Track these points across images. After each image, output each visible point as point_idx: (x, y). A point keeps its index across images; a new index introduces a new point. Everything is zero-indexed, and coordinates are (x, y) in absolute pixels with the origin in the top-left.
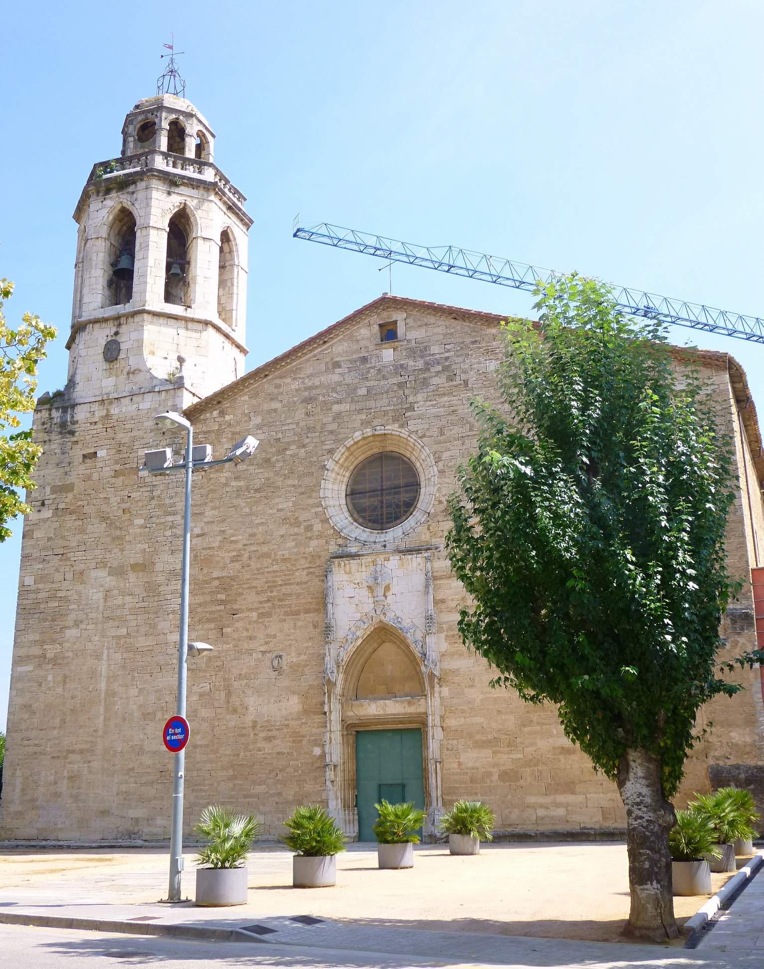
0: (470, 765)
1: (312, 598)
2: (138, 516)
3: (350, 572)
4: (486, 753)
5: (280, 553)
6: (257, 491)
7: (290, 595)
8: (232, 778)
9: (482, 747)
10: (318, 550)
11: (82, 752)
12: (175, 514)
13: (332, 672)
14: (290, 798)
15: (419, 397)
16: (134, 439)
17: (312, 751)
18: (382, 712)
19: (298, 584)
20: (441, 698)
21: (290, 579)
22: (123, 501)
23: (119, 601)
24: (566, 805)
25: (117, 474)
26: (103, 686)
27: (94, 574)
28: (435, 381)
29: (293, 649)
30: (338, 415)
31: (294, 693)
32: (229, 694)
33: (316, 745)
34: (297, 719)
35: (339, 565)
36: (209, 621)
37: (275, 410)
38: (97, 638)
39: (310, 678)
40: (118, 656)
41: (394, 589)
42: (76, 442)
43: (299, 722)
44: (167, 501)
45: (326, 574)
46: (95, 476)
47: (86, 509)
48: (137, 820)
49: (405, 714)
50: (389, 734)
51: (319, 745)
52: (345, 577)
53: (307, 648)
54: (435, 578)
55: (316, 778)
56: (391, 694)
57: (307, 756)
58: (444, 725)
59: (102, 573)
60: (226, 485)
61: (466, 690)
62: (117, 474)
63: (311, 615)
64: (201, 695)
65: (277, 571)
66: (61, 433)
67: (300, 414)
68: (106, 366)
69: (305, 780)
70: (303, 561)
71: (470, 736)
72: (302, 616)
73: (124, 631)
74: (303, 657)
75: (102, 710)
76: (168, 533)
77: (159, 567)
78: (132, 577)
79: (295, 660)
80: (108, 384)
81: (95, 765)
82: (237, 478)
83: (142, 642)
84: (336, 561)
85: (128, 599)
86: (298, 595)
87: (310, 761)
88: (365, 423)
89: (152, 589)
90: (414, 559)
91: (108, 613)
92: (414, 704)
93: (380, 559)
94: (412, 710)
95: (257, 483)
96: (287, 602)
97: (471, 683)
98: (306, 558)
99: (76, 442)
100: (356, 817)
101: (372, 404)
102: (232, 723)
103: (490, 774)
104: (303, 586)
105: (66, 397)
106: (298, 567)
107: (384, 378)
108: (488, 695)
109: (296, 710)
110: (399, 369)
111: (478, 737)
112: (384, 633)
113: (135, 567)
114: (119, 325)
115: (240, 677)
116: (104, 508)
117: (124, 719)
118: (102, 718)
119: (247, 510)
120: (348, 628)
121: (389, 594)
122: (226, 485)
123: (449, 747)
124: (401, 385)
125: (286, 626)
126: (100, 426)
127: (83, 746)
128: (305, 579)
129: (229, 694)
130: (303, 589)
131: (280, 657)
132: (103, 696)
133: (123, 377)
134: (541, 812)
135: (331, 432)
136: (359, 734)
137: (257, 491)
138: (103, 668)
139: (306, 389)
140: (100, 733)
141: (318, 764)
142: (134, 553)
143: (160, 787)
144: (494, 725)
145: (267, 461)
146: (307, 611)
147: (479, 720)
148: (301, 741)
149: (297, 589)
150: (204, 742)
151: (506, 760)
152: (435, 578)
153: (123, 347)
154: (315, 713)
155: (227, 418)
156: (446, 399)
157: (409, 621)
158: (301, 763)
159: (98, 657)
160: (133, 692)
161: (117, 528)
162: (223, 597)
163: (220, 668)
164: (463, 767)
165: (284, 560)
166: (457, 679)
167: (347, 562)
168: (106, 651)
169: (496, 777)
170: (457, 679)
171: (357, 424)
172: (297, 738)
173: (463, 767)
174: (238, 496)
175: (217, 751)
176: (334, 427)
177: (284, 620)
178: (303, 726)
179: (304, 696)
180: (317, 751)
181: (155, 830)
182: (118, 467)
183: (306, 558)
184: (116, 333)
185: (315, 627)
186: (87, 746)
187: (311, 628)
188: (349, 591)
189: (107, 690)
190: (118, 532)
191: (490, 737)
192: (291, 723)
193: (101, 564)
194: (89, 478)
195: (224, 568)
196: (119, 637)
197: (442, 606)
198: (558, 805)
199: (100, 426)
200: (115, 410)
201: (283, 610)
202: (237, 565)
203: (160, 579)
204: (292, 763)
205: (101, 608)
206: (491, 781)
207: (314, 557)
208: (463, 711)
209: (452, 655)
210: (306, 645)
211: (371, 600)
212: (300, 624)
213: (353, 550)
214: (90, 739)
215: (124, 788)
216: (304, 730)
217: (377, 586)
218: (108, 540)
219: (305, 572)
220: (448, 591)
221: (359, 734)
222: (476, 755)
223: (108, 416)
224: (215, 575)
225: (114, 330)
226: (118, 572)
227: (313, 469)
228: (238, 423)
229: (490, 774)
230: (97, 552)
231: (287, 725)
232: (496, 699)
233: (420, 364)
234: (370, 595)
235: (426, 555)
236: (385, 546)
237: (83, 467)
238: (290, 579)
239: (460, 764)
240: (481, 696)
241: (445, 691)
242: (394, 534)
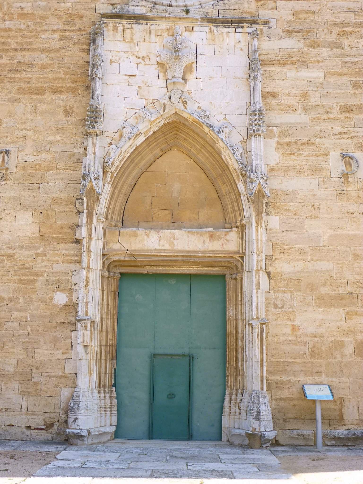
0: (311, 330)
1: (66, 73)
3: (132, 40)
5: (18, 5)
7: (30, 65)
9: (330, 305)
10: (78, 7)
13: (97, 178)
14: (10, 369)
17: (52, 298)
18: (167, 247)
19: (44, 51)
20: (269, 231)
21: (31, 43)
29: (29, 143)
31: (26, 208)
33: (58, 289)
34: (28, 248)
35: (115, 28)
39: (56, 187)
41: (201, 70)
43: (32, 253)
45: (93, 38)
49: (205, 252)
50: (172, 282)
51: (64, 290)
52: (124, 46)
53: (52, 143)
54: (264, 63)
55: (55, 340)
56: (177, 223)
57: (43, 305)
58: (272, 270)
61: (307, 222)
63: (62, 97)
65: (10, 30)
69: (37, 342)
70: (54, 20)
71: (312, 288)
72: (47, 96)
74: (44, 156)
79: (31, 159)
84: (111, 22)
86: (43, 67)
87: (49, 313)
90: (232, 34)
92: (219, 238)
93: (180, 27)
94: (215, 246)
96: (24, 75)
97: (314, 213)
98: (60, 17)
100: (115, 402)
103: (340, 345)
104: (54, 55)
106: (47, 28)
108: (339, 232)
109: (29, 234)
111: (324, 290)
112: (178, 132)
120: (123, 118)
121: (191, 77)
123: (278, 302)
125: (20, 109)
130: (52, 59)
131: (7, 152)
136: (127, 277)
141: (61, 319)
144: (349, 275)
146: (56, 91)
147: (326, 265)
148: (33, 282)
149: (44, 58)
152: (264, 63)
154: (60, 240)
157: (220, 117)
158: (32, 316)
164: (300, 333)
165: (23, 16)
166: (292, 205)
167: (127, 26)
169: (349, 350)
170: (292, 205)
172: (27, 277)
173: (300, 333)
177: (17, 100)
178: (39, 259)
179: (43, 214)
180: (61, 298)
183: (60, 17)
185: (68, 113)
187: (61, 115)
188: (128, 66)
191: (342, 291)
192: (18, 253)
197: (273, 102)
201: (16, 86)
204: (15, 314)
206: (343, 356)
208: (301, 252)
209: (286, 170)
210: (51, 138)
211: (162, 83)
212: (43, 107)
216: (40, 265)
217: (174, 62)
219: (56, 36)
220: (282, 82)
221: (127, 277)
222: (320, 317)
229: (340, 345)
231: (11, 257)
232: (351, 238)
234: (161, 75)
235: (250, 30)
236: (187, 12)
238: (31, 43)
239: (294, 328)
240: (330, 232)
241: (274, 221)
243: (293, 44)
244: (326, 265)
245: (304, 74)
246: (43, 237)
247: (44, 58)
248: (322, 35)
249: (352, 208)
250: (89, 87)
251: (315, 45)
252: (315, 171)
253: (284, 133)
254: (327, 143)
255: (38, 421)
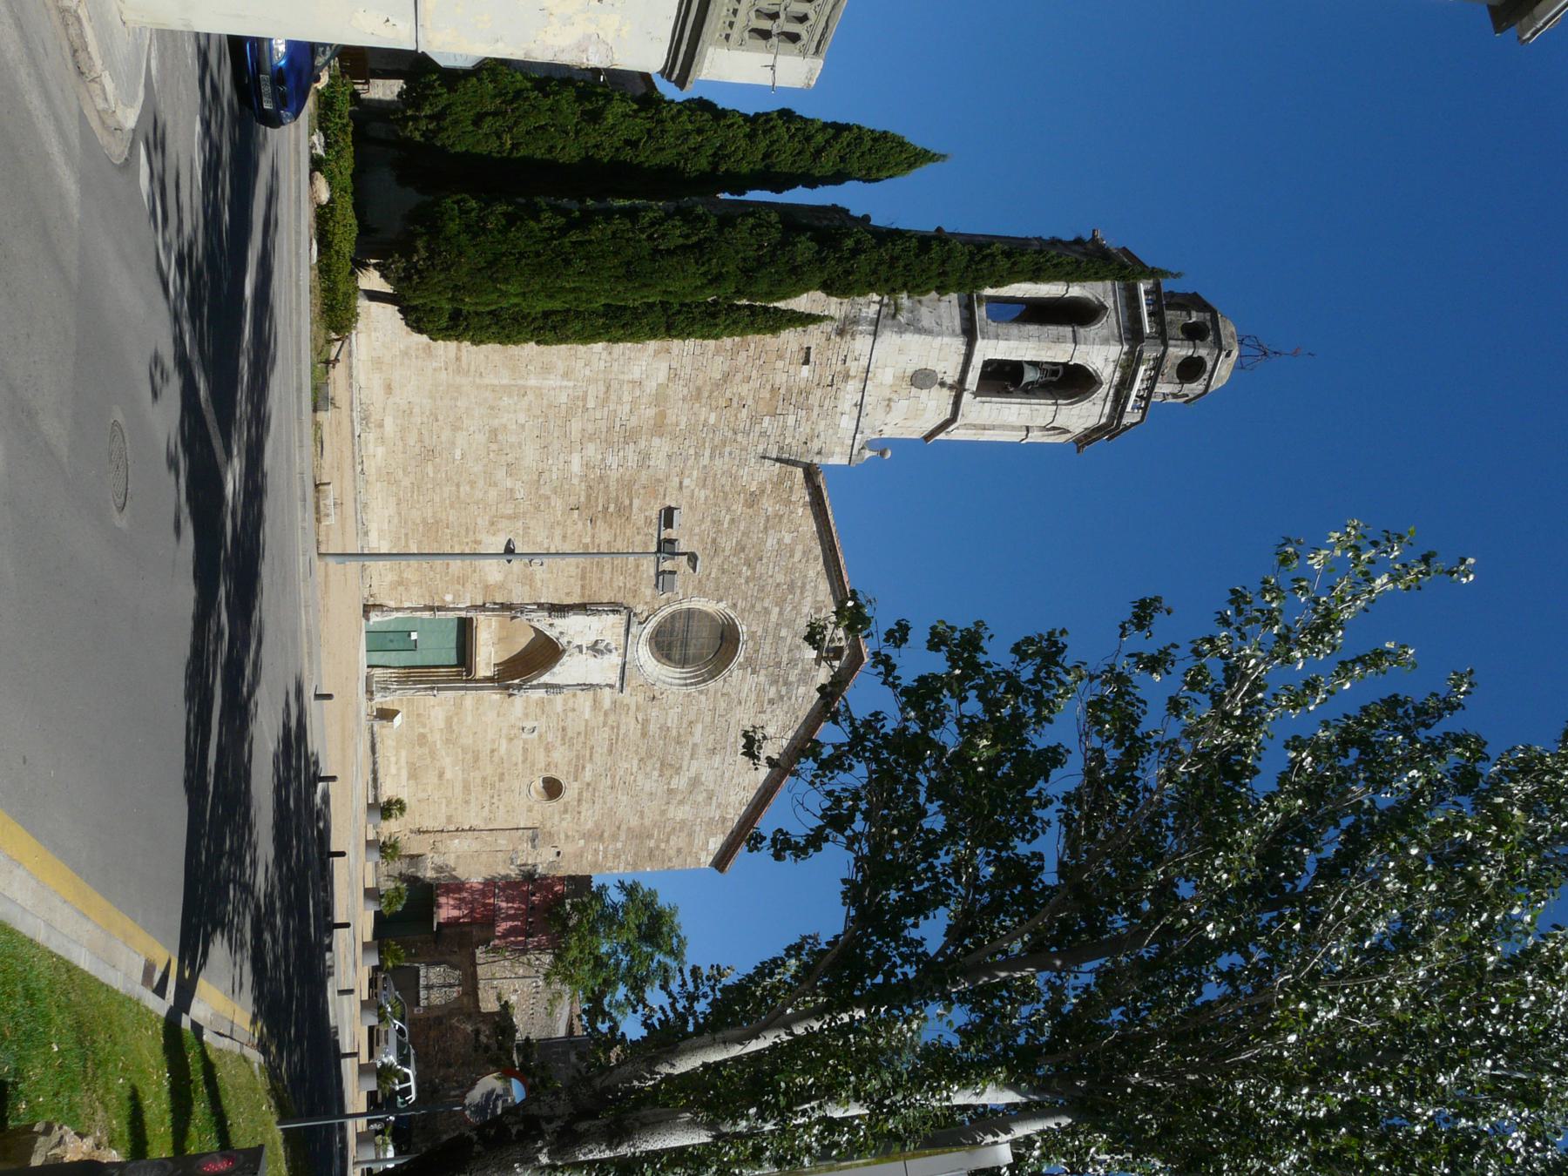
2: (719, 419)
4: (442, 725)
6: (714, 541)
8: (424, 521)
11: (458, 359)
12: (712, 457)
15: (762, 679)
16: (809, 409)
22: (741, 398)
23: (627, 398)
24: (398, 775)
25: (774, 390)
26: (532, 382)
27: (664, 366)
28: (773, 690)
30: (767, 611)
32: (509, 517)
36: (588, 497)
37: (792, 556)
38: (587, 373)
40: (564, 399)
42: (829, 339)
44: (728, 449)
46: (780, 364)
47: (743, 354)
48: (381, 426)
52: (609, 624)
59: (662, 376)
60: (729, 510)
62: (774, 390)
64: (511, 490)
66: (846, 317)
67: (780, 578)
68: (910, 372)
73: (591, 404)
75: (505, 382)
76: (692, 451)
77: (656, 441)
78: (651, 412)
80: (885, 376)
81: (443, 375)
82: (732, 521)
83: (576, 426)
85: (627, 408)
88: (752, 635)
89: (631, 436)
91: (615, 385)
95: (722, 541)
99: (829, 339)
101: (769, 640)
102: (479, 521)
103: (424, 726)
105: (890, 322)
107: (790, 650)
110: (792, 662)
113: (662, 415)
114: (951, 387)
115: (526, 528)
116: (739, 376)
117: (492, 408)
118: (496, 382)
119: (697, 530)
122: (729, 510)
124: (778, 664)
126: (839, 367)
127: (464, 359)
128: (615, 585)
129: (509, 517)
132: (520, 382)
133: (887, 393)
134: (393, 759)
135: (753, 606)
137: (714, 541)
138: (553, 381)
139: (803, 587)
140: (478, 381)
142: (679, 415)
143: (417, 450)
145: (743, 549)
147: (469, 719)
149: (607, 577)
150: (462, 495)
151: (437, 738)
153: (925, 392)
155: (800, 511)
156: (753, 697)
159: (566, 375)
160: (522, 419)
161: (711, 392)
162: (612, 509)
163: (537, 508)
168: (571, 384)
171: (754, 628)
174: (714, 522)
175: (452, 506)
176: (758, 607)
179: (501, 586)
181: (371, 446)
182: (782, 391)
184: (942, 384)
186: (464, 365)
189: (525, 387)
190: (706, 394)
193: (674, 375)
194: (781, 357)
195: (640, 509)
196: (585, 399)
198: (399, 769)
199: (839, 367)
200: (853, 386)
202: (641, 523)
203: (643, 444)
205: (621, 377)
207: (635, 593)
213: (633, 630)
214: (473, 368)
215: (416, 410)
216: (469, 586)
217: (596, 649)
218: (699, 383)
223: (847, 377)
224: (636, 502)
225: (949, 381)
226: (660, 398)
227: (722, 591)
228: (791, 521)
229: (424, 726)
230: (688, 370)
233: (792, 678)
237: (796, 347)
242: (643, 654)
243: (607, 704)
244: (469, 719)
245: (587, 710)
246: (487, 587)
247: (607, 577)
248: (612, 719)
249: (504, 732)
250: (583, 608)
251: (606, 714)
252: (526, 715)
253: (550, 701)
254: (544, 719)
255: (375, 590)
